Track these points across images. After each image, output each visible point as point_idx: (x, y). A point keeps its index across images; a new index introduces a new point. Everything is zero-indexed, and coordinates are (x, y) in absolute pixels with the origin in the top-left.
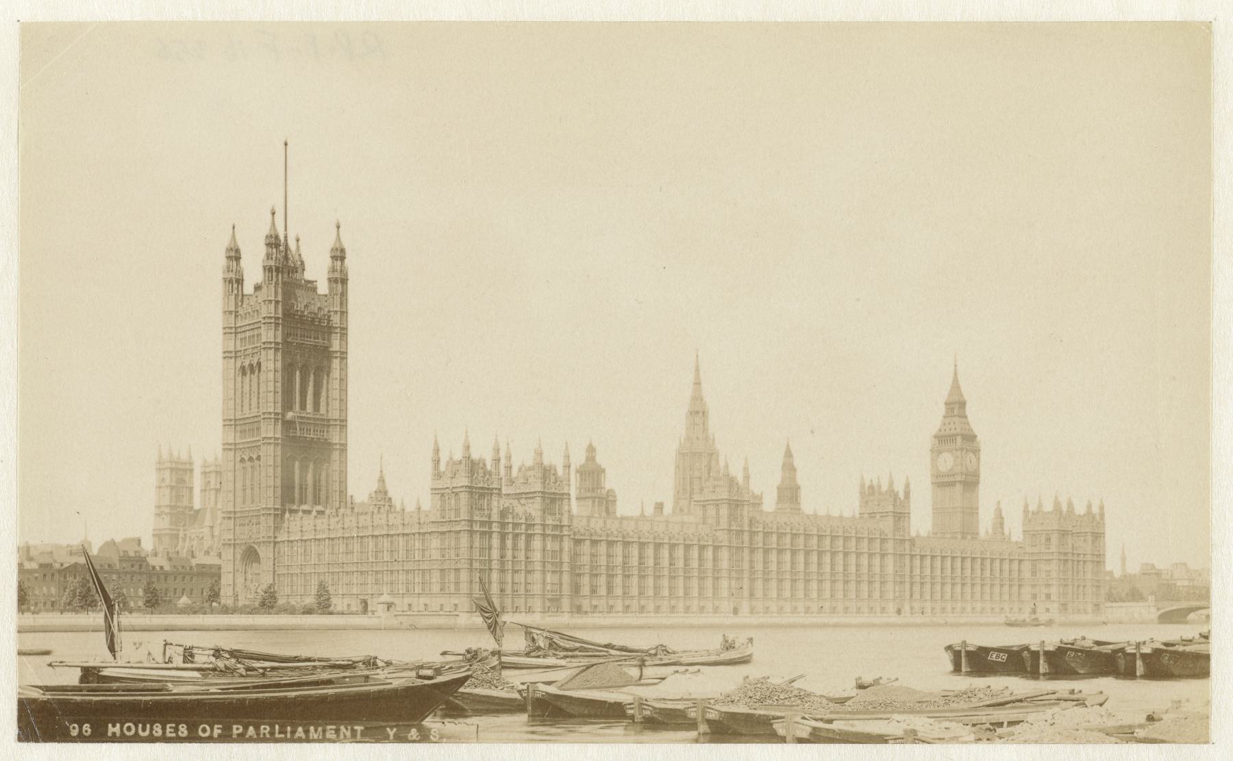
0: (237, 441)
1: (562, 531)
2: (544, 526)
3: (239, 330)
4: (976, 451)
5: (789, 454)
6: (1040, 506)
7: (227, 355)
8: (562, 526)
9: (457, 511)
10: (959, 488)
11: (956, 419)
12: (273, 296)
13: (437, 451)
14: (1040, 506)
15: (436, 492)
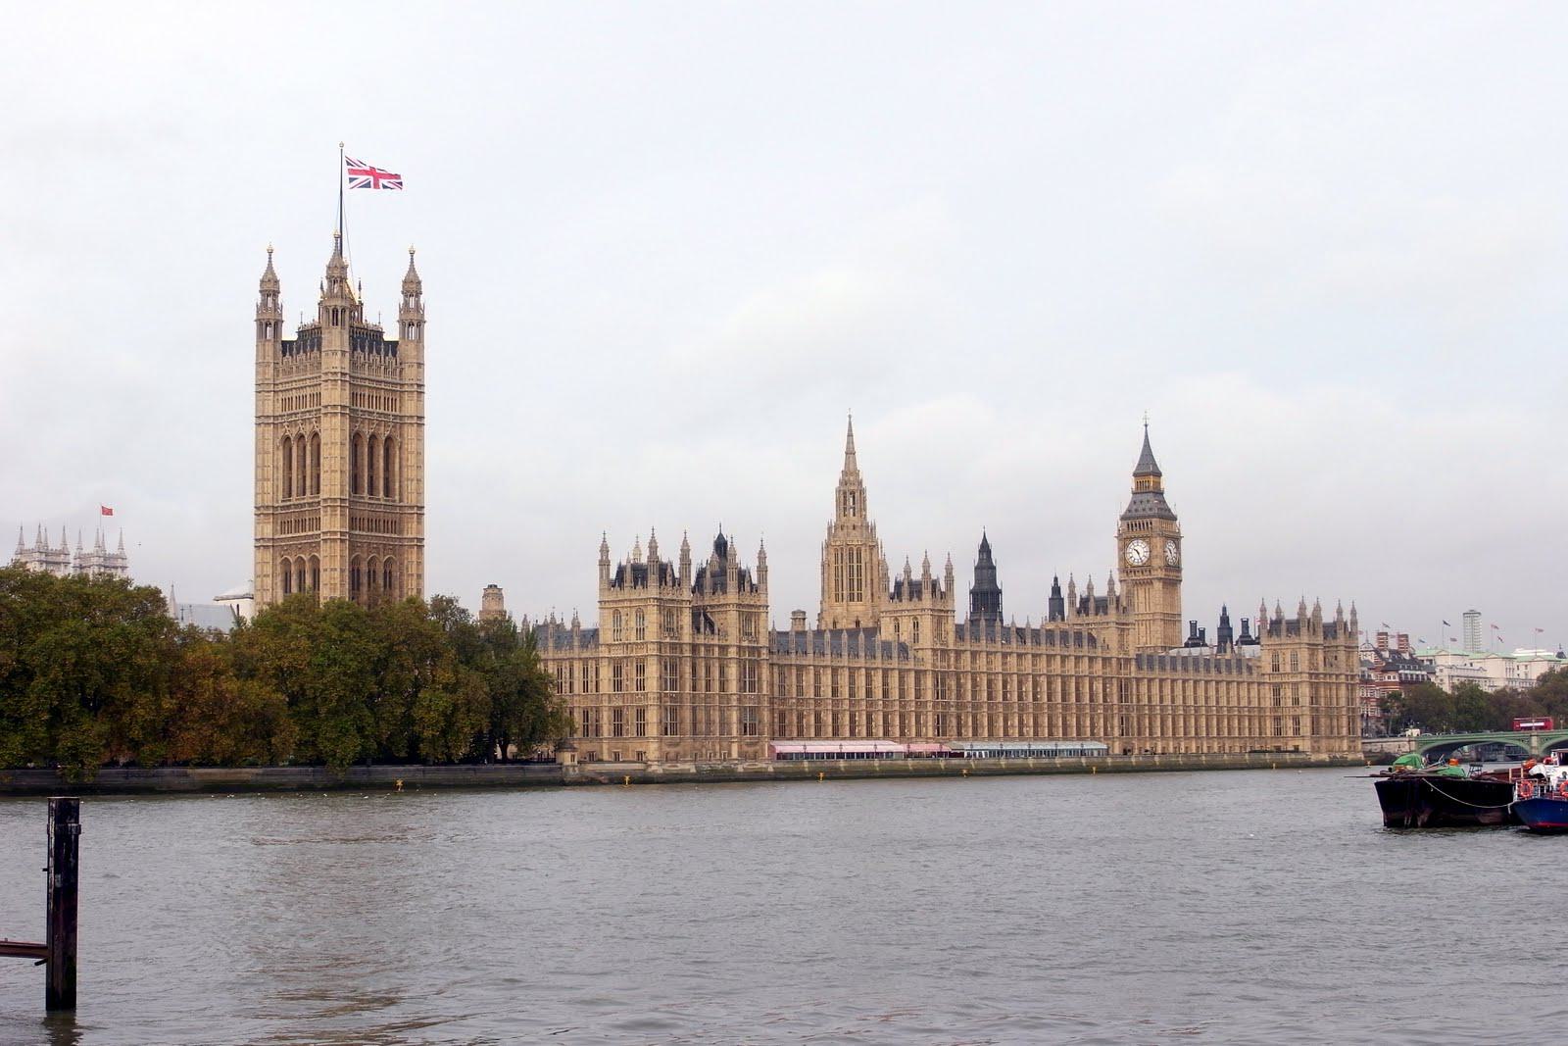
0: (276, 537)
1: (759, 656)
2: (739, 647)
3: (280, 388)
4: (1176, 539)
5: (985, 549)
6: (1278, 611)
7: (262, 420)
8: (758, 650)
9: (641, 631)
10: (1158, 585)
11: (1150, 496)
12: (338, 343)
13: (604, 550)
14: (1278, 611)
15: (607, 605)
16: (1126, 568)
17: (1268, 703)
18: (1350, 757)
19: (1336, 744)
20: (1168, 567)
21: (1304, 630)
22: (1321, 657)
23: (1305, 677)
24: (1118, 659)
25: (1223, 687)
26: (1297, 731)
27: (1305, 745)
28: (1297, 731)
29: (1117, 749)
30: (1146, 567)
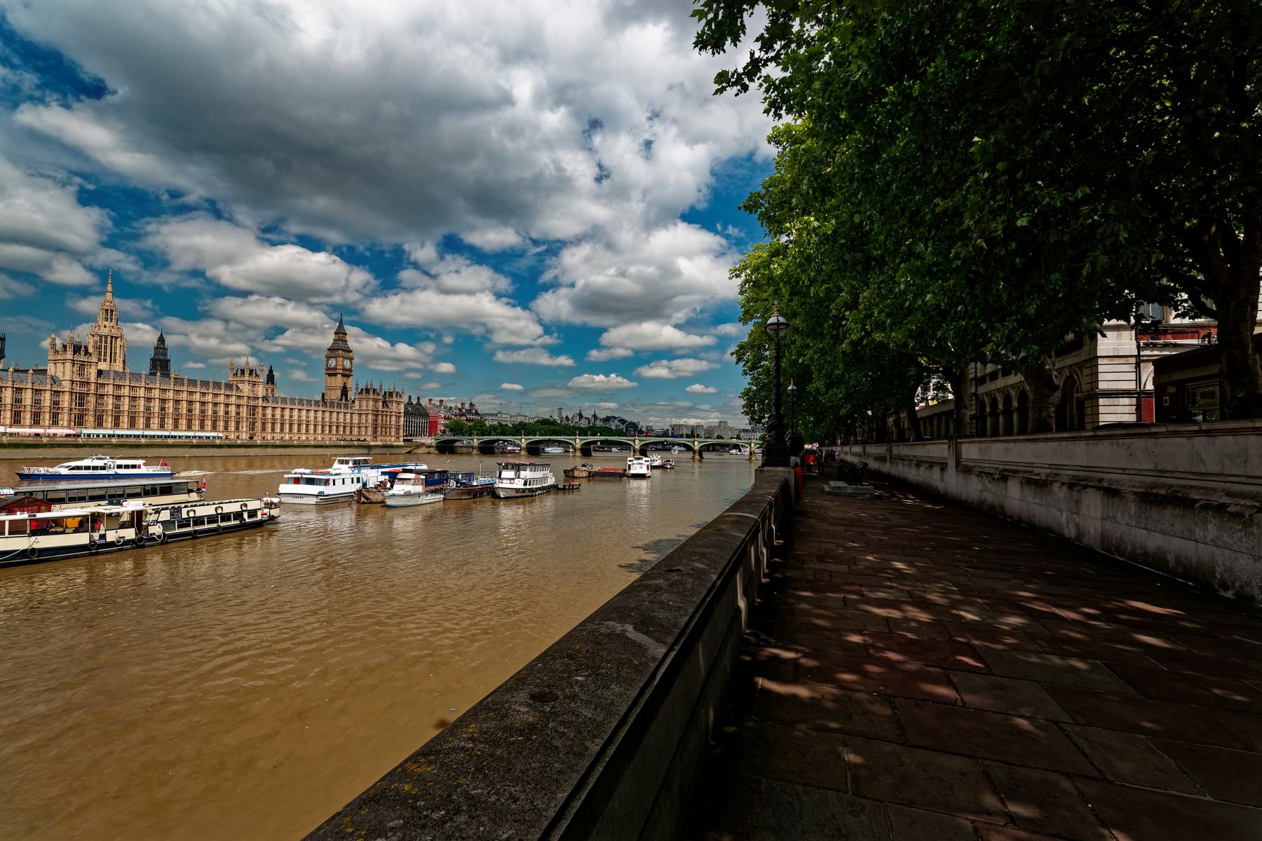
10: (339, 376)
16: (328, 369)
17: (356, 420)
18: (395, 444)
19: (388, 439)
20: (344, 369)
21: (371, 393)
22: (381, 404)
23: (370, 412)
24: (249, 397)
25: (327, 414)
26: (366, 432)
27: (368, 438)
28: (366, 432)
29: (245, 436)
30: (335, 369)
